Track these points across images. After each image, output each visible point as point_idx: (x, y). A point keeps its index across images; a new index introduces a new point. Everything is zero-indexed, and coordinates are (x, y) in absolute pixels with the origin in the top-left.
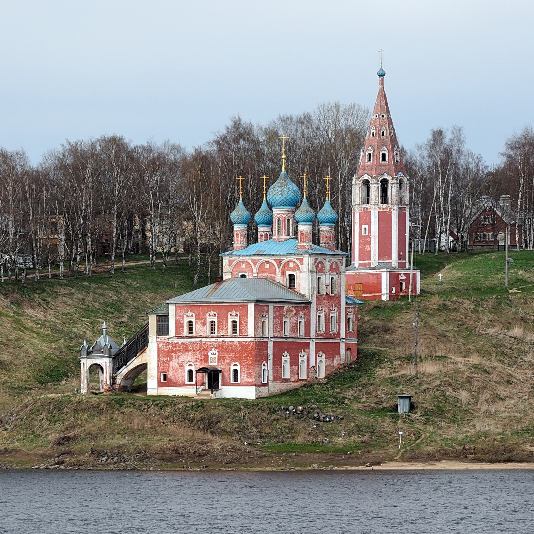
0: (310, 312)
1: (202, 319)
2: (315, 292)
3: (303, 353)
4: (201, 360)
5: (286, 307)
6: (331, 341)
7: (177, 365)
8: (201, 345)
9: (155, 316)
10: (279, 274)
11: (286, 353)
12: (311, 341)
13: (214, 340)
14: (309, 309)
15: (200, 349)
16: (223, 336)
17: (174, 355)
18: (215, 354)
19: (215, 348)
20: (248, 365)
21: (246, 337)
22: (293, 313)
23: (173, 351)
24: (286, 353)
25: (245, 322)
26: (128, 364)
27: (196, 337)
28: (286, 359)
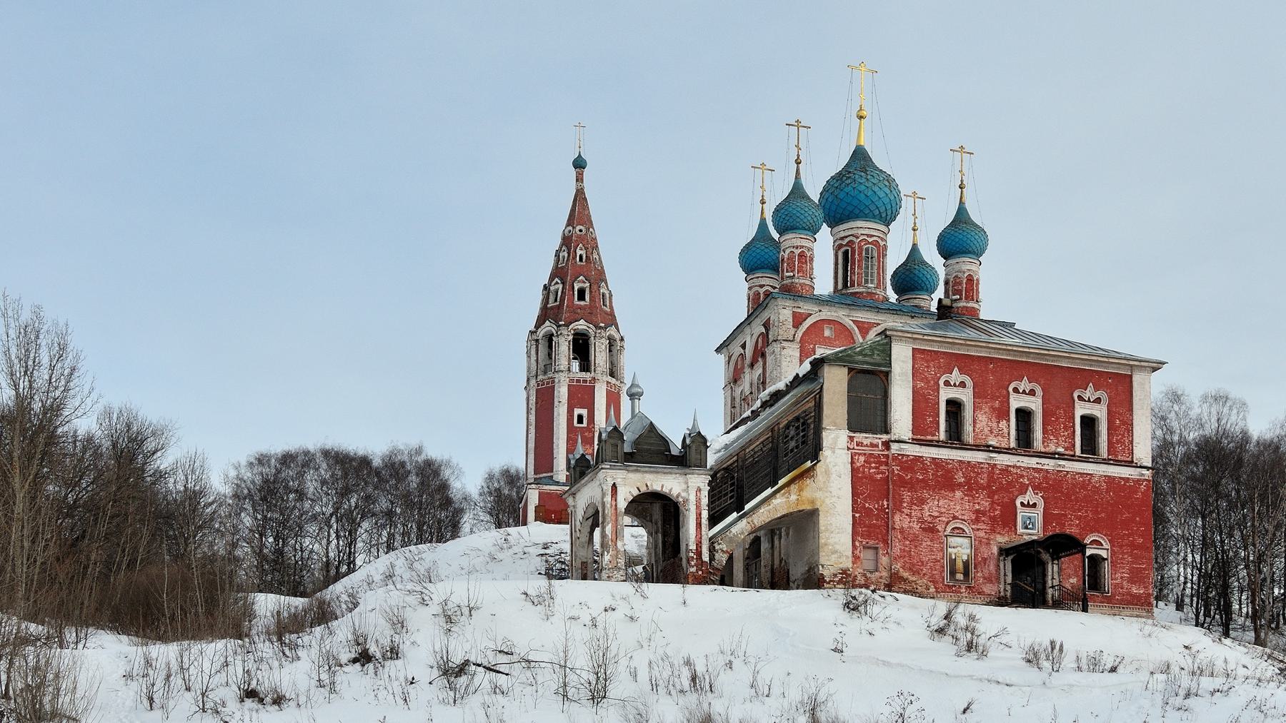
1: (994, 398)
4: (993, 519)
7: (916, 526)
8: (991, 474)
9: (846, 370)
13: (1033, 462)
15: (989, 486)
16: (1061, 457)
17: (907, 495)
18: (1034, 505)
19: (1037, 488)
20: (1133, 546)
21: (1130, 464)
23: (902, 483)
25: (1123, 422)
26: (747, 507)
27: (977, 448)
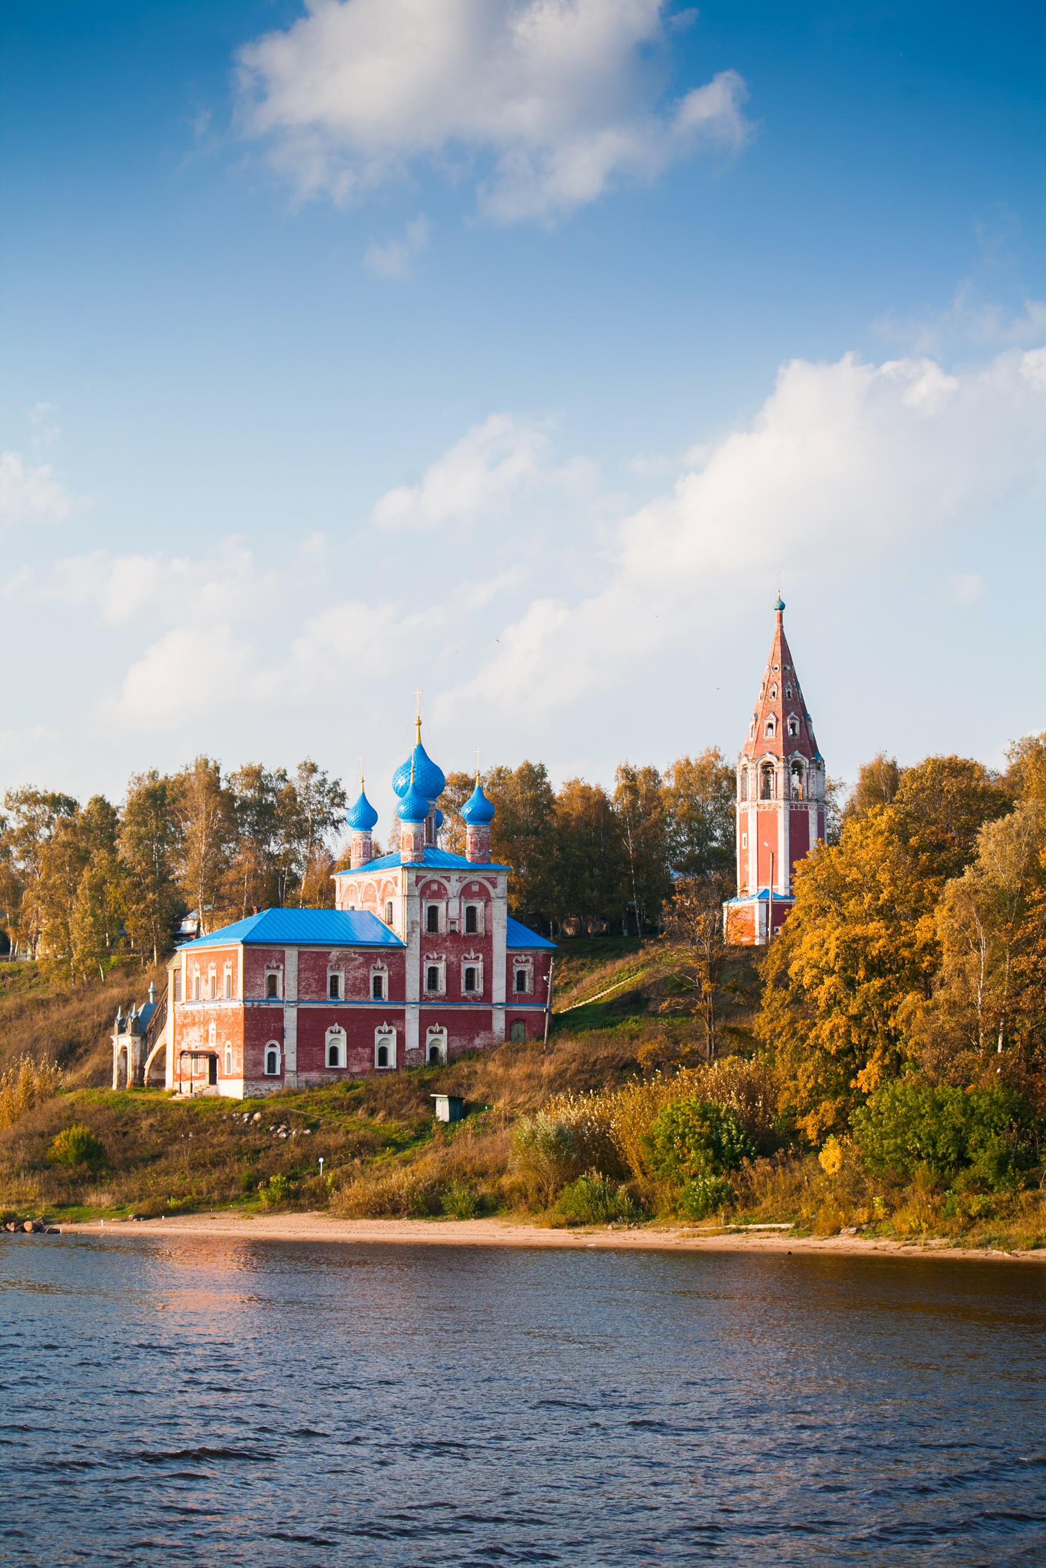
0: (404, 962)
2: (418, 930)
3: (385, 1027)
5: (335, 953)
6: (465, 1008)
10: (379, 902)
11: (336, 1027)
12: (407, 1008)
14: (403, 958)
22: (357, 963)
24: (336, 1027)
28: (338, 1039)
